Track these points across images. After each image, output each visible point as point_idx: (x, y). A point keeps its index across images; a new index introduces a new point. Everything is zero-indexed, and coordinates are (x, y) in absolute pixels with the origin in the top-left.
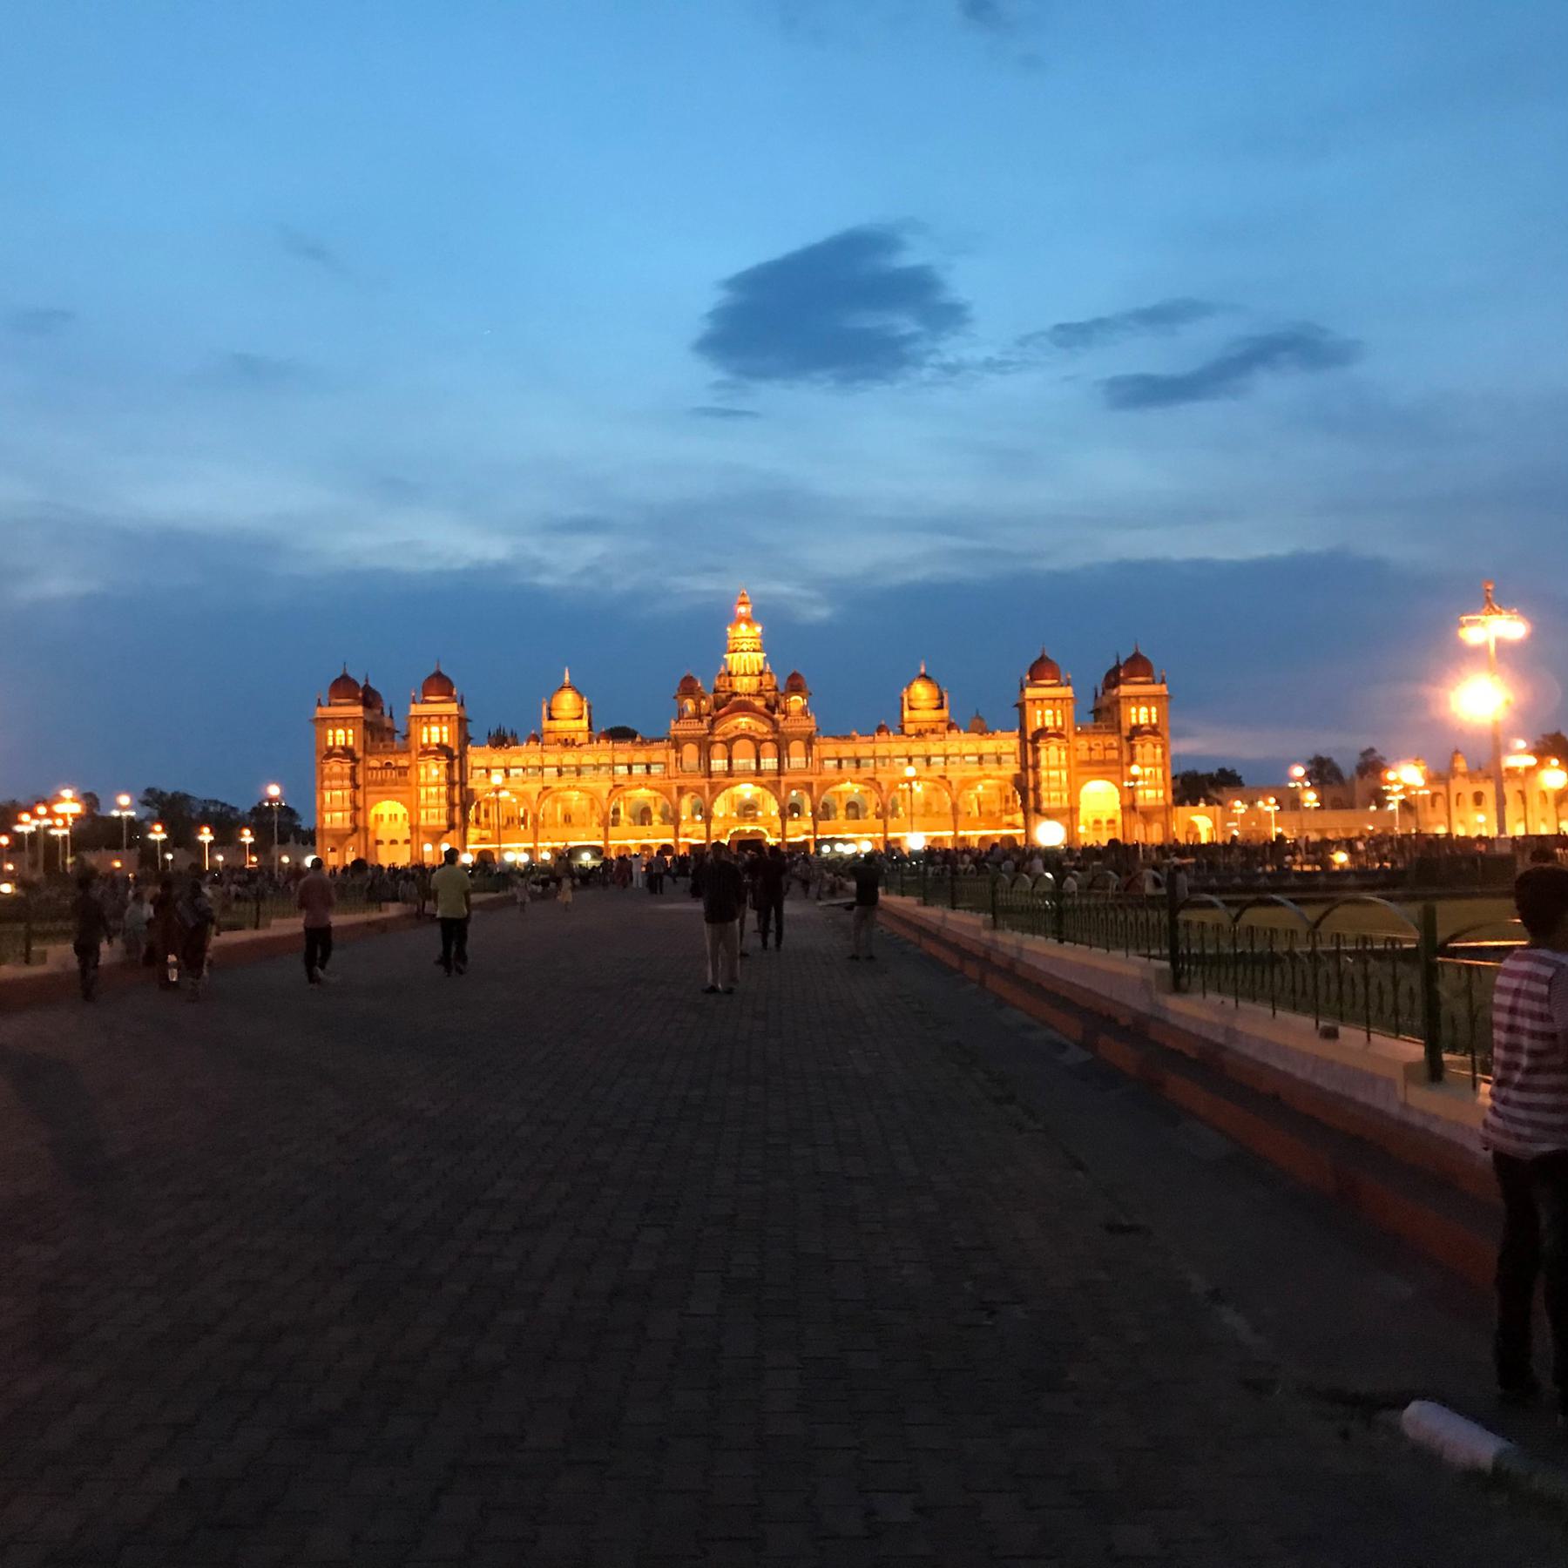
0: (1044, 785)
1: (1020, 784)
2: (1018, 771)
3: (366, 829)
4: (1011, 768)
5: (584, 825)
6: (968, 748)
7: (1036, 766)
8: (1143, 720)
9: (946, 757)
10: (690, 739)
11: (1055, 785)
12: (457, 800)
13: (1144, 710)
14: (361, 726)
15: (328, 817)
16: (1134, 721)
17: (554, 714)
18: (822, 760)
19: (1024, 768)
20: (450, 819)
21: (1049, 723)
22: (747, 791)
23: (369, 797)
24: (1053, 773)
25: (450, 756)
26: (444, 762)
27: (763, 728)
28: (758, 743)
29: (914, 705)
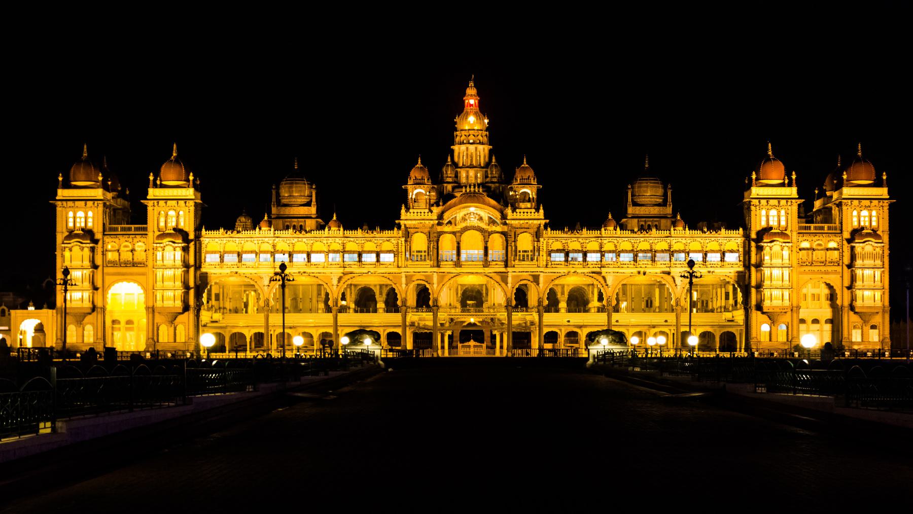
0: (767, 283)
1: (743, 282)
2: (741, 269)
3: (104, 309)
5: (311, 311)
7: (759, 265)
8: (865, 222)
12: (192, 284)
13: (865, 213)
14: (101, 208)
16: (855, 224)
18: (549, 253)
19: (747, 265)
21: (773, 223)
23: (107, 278)
24: (776, 272)
25: (186, 239)
26: (180, 243)
28: (486, 234)
29: (639, 200)
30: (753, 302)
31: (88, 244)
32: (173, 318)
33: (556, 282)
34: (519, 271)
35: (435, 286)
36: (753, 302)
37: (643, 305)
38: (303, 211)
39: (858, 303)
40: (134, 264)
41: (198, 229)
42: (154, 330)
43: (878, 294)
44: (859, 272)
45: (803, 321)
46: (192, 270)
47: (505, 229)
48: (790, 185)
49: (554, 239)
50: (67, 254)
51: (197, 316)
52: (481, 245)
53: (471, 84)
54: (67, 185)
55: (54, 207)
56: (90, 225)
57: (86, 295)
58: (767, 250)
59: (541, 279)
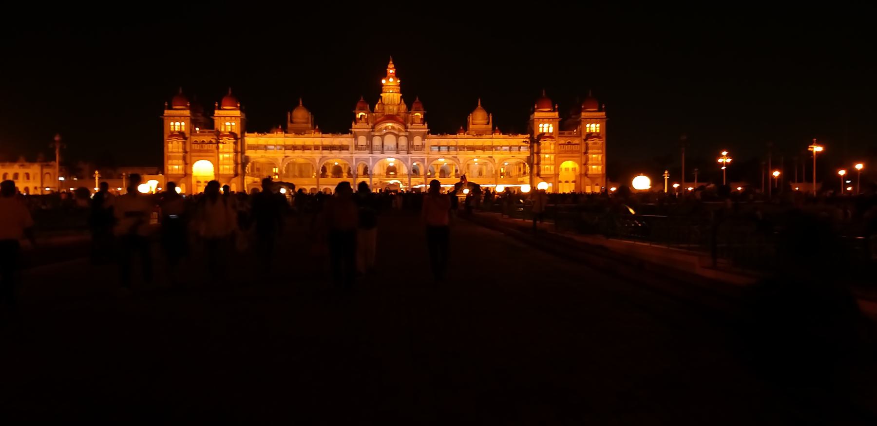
0: (542, 162)
1: (530, 161)
3: (191, 175)
4: (525, 153)
7: (538, 153)
10: (362, 134)
11: (549, 162)
12: (239, 161)
14: (189, 121)
15: (170, 167)
17: (294, 120)
19: (532, 154)
20: (236, 170)
23: (193, 158)
24: (547, 156)
26: (232, 140)
28: (397, 136)
29: (475, 122)
31: (181, 140)
33: (434, 162)
34: (416, 155)
35: (371, 164)
36: (535, 171)
39: (590, 172)
41: (242, 133)
43: (600, 168)
44: (590, 156)
45: (560, 182)
46: (239, 154)
47: (407, 134)
48: (554, 111)
49: (434, 140)
50: (170, 145)
52: (395, 144)
53: (391, 62)
54: (170, 108)
55: (162, 121)
56: (183, 129)
57: (181, 167)
58: (542, 145)
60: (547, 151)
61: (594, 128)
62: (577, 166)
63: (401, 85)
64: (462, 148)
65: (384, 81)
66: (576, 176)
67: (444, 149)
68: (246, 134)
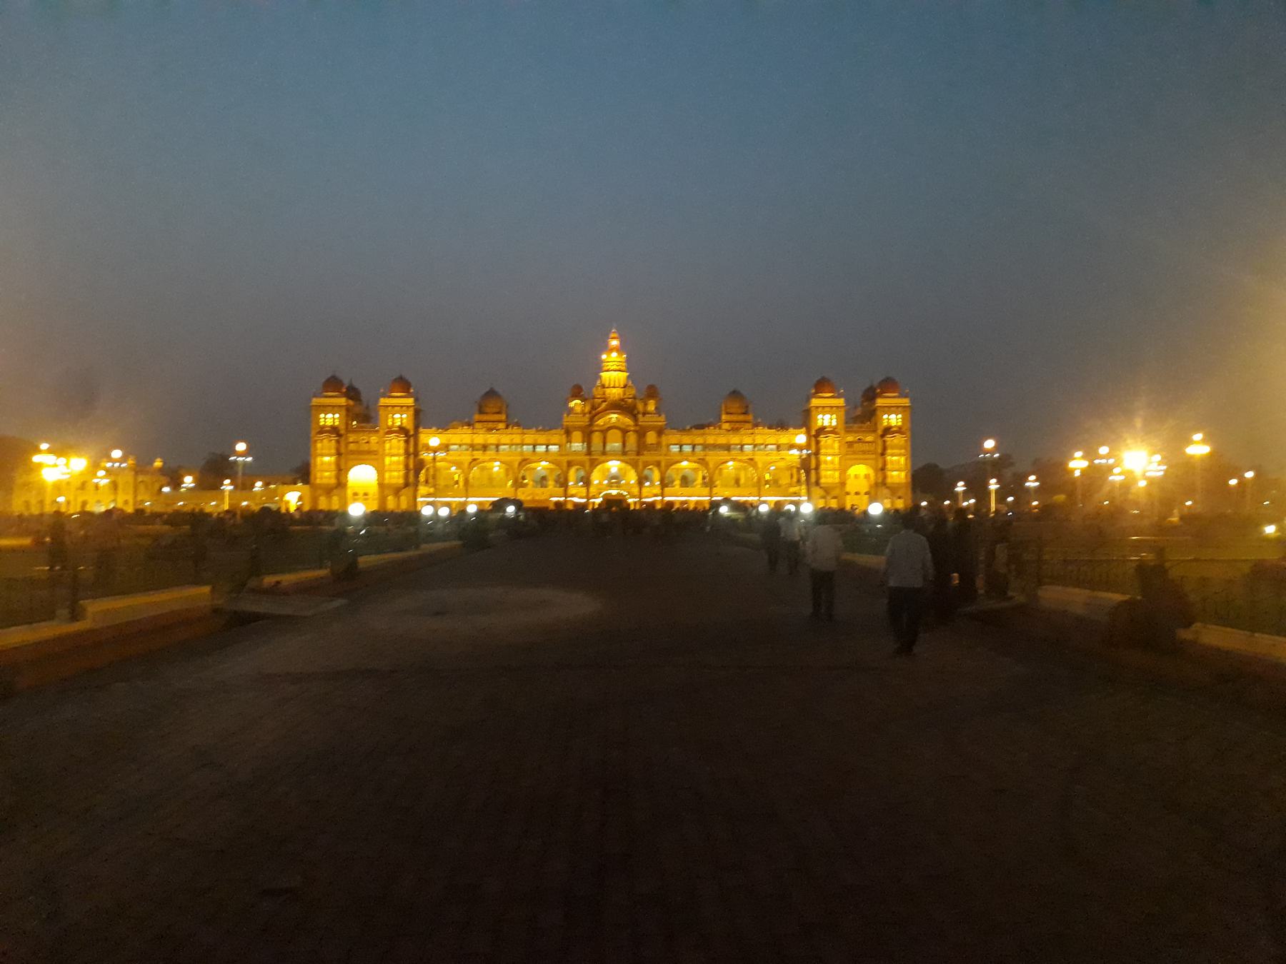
0: (823, 466)
6: (771, 440)
9: (755, 446)
11: (830, 466)
14: (344, 412)
15: (318, 475)
18: (668, 446)
20: (406, 476)
22: (614, 466)
24: (829, 458)
26: (402, 438)
27: (628, 421)
28: (625, 432)
30: (813, 479)
32: (397, 491)
34: (647, 457)
37: (733, 482)
38: (497, 417)
39: (889, 480)
40: (369, 452)
41: (416, 428)
42: (383, 500)
43: (903, 474)
45: (848, 494)
50: (319, 445)
51: (416, 490)
56: (337, 423)
59: (663, 464)
60: (830, 451)
61: (894, 420)
62: (871, 472)
63: (627, 361)
64: (715, 447)
65: (604, 357)
66: (871, 487)
67: (687, 449)
68: (421, 430)
